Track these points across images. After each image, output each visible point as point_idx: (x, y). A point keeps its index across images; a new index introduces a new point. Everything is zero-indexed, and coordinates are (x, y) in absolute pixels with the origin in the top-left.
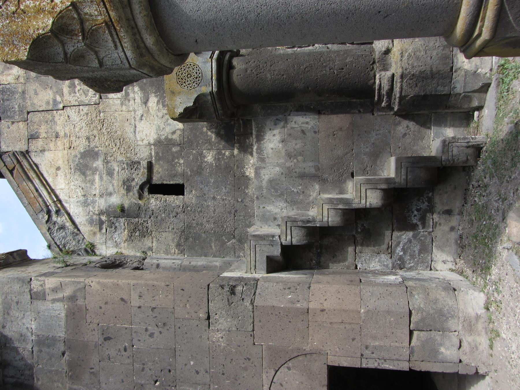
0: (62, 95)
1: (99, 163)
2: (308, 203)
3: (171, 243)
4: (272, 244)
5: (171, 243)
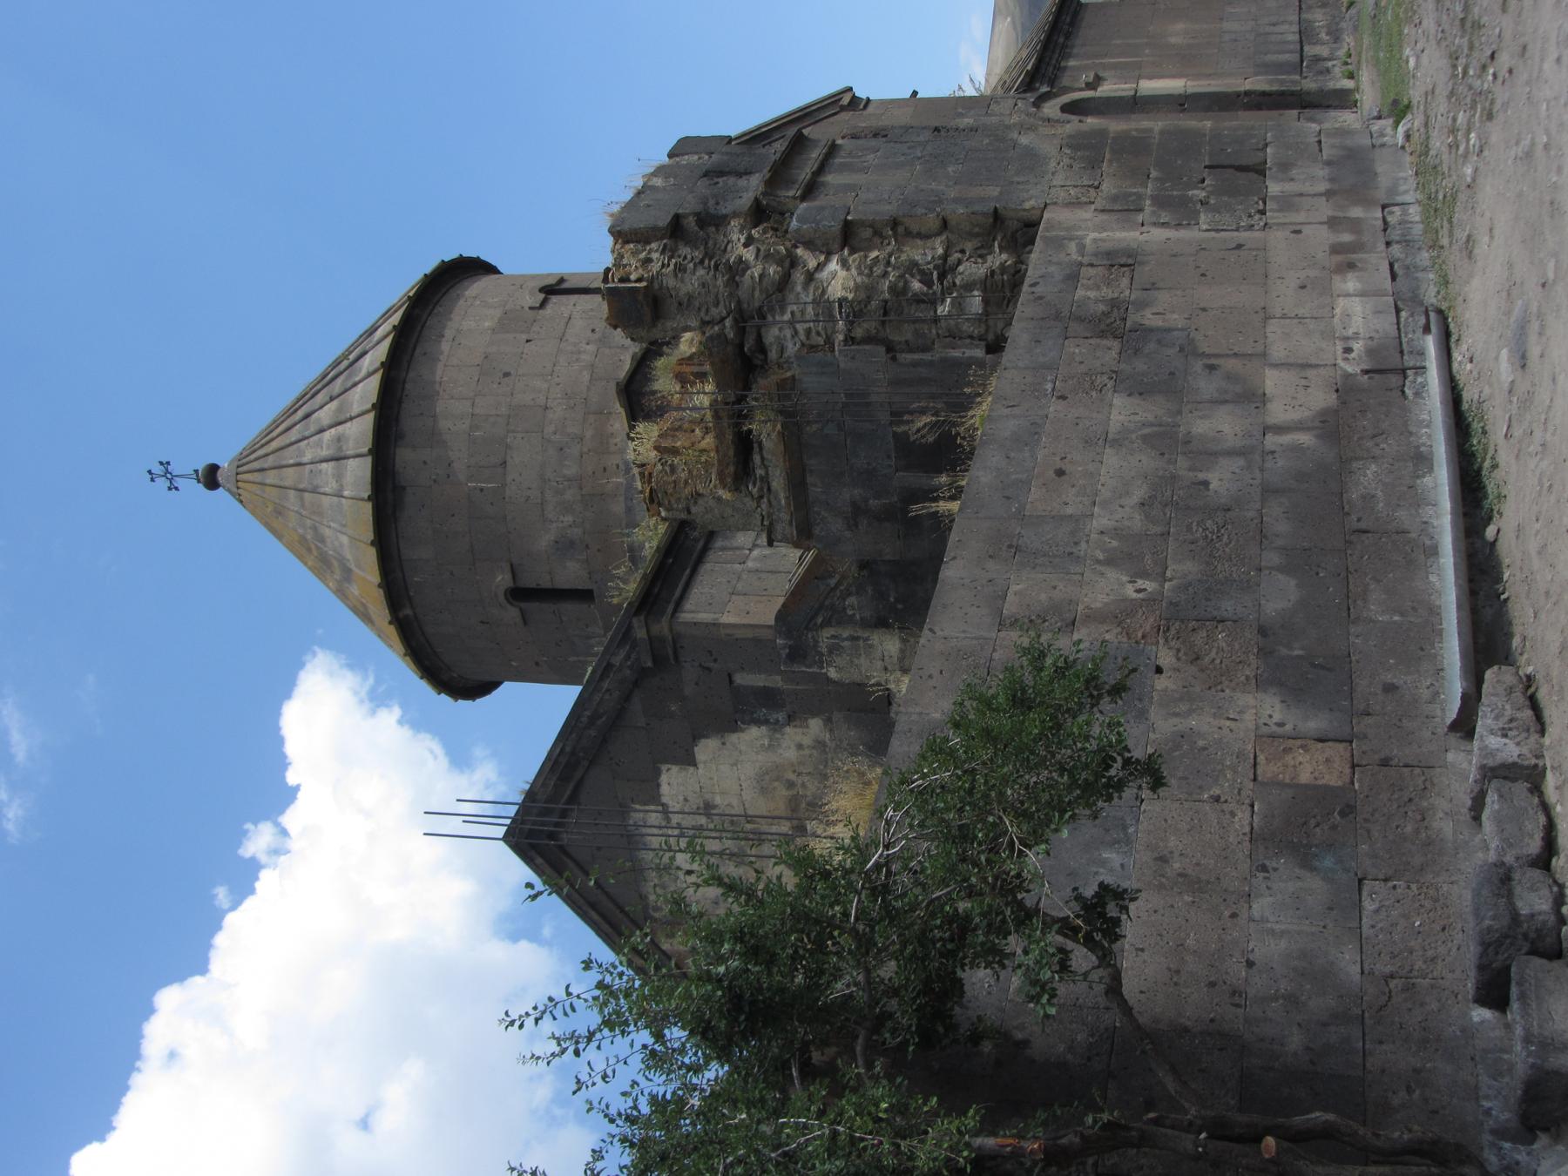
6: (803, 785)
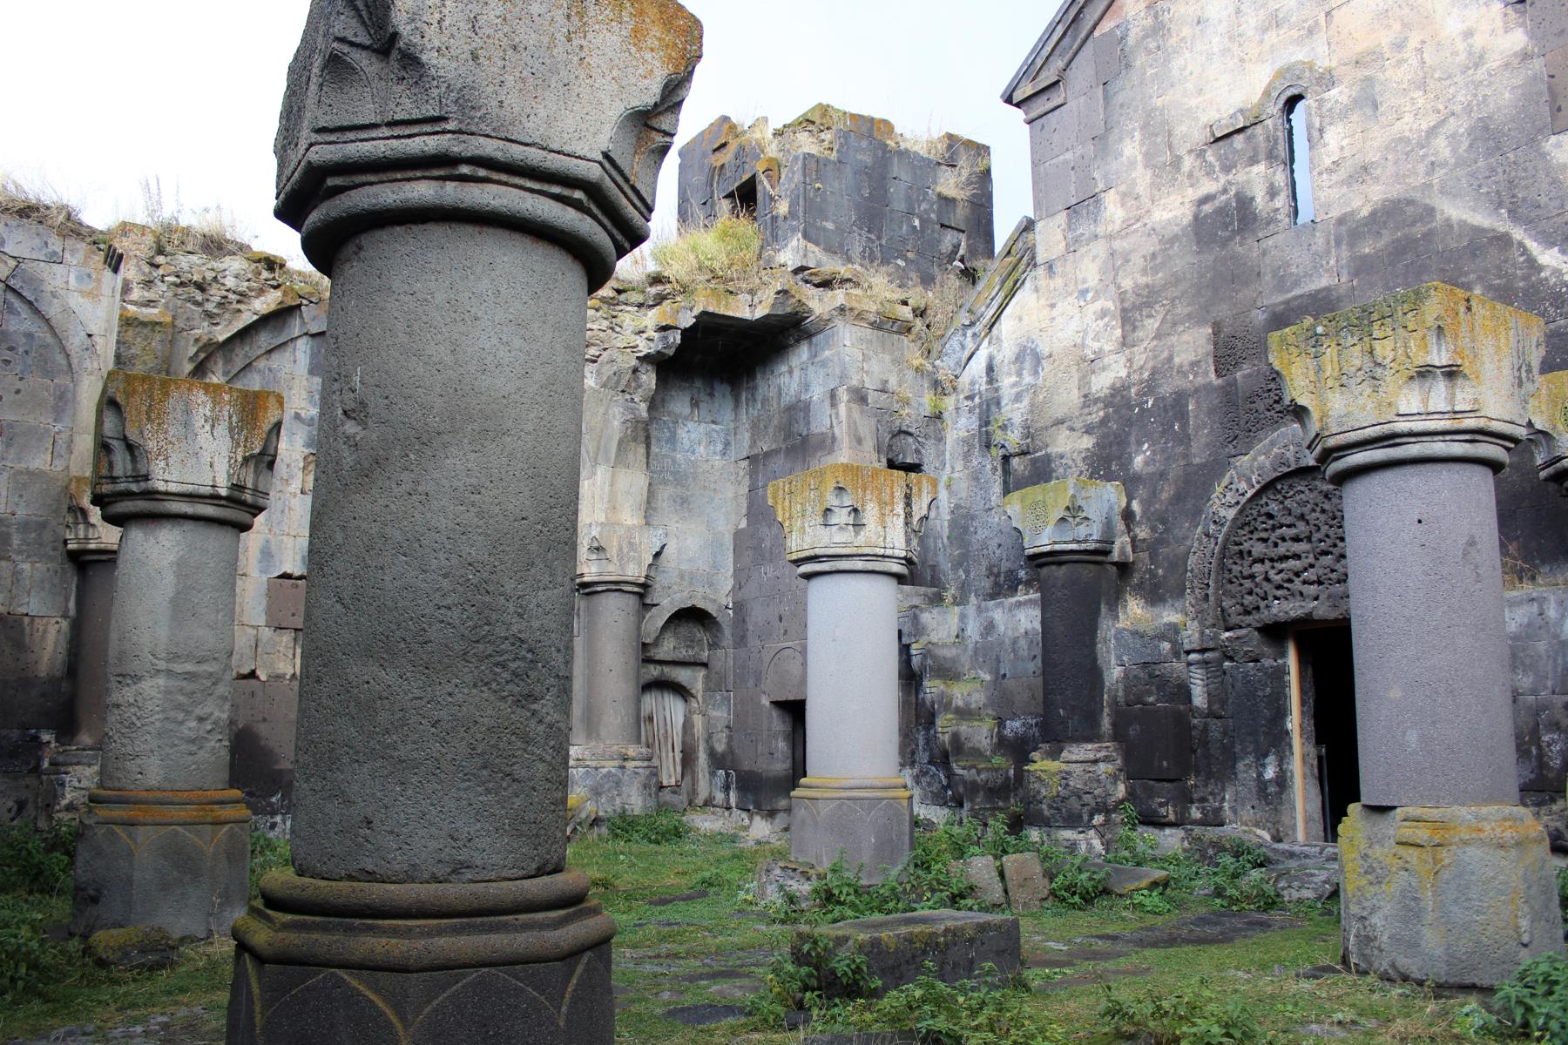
0: (1094, 300)
1: (1028, 379)
6: (1400, 62)
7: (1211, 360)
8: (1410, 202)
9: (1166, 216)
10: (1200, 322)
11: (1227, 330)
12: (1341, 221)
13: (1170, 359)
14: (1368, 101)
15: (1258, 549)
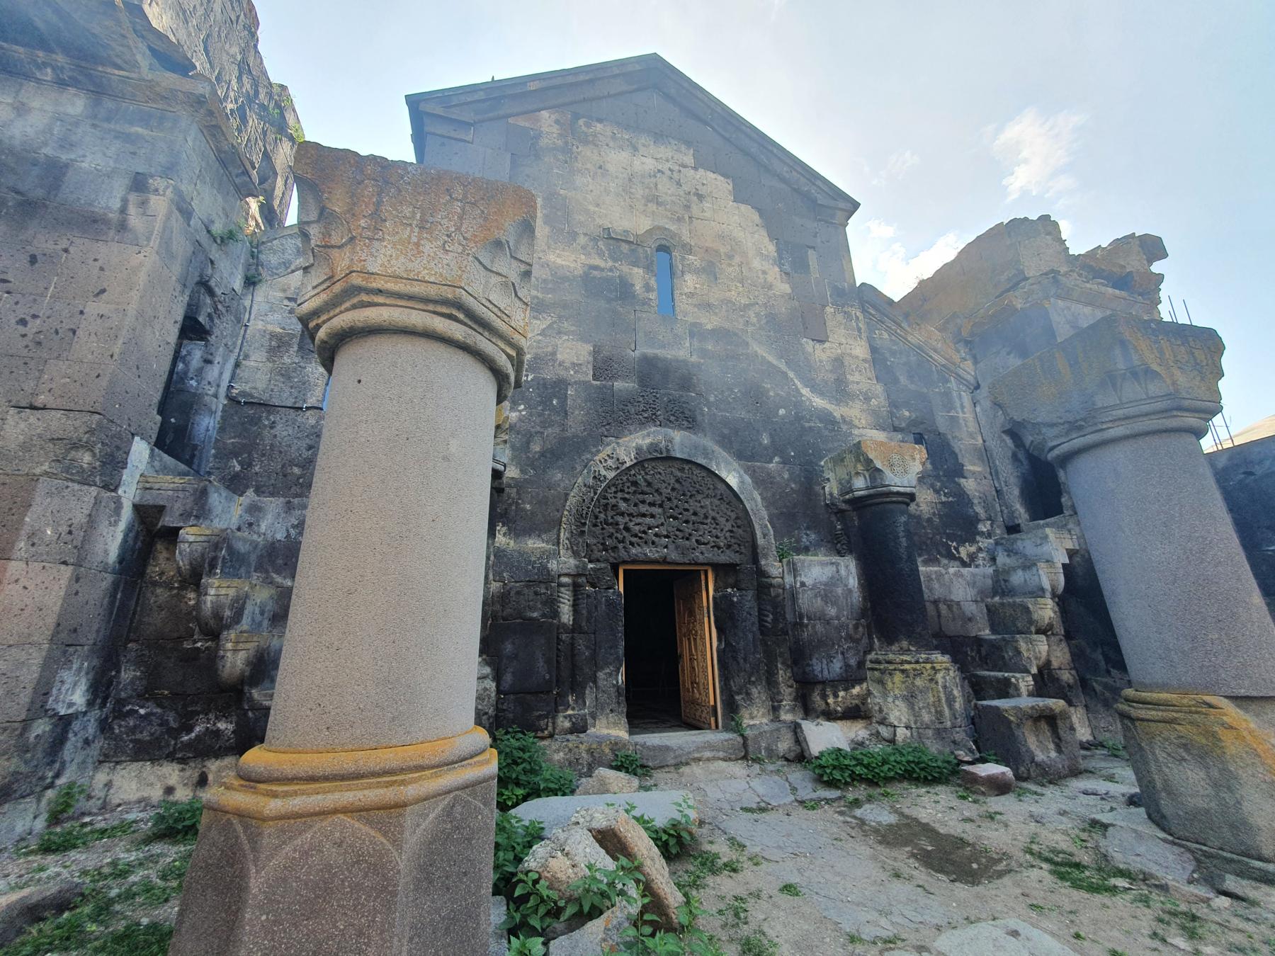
2: (267, 572)
3: (250, 385)
4: (186, 515)
5: (250, 385)
6: (730, 265)
7: (590, 367)
8: (736, 334)
9: (559, 261)
10: (583, 339)
11: (605, 353)
12: (694, 325)
13: (554, 354)
14: (710, 271)
15: (623, 506)
